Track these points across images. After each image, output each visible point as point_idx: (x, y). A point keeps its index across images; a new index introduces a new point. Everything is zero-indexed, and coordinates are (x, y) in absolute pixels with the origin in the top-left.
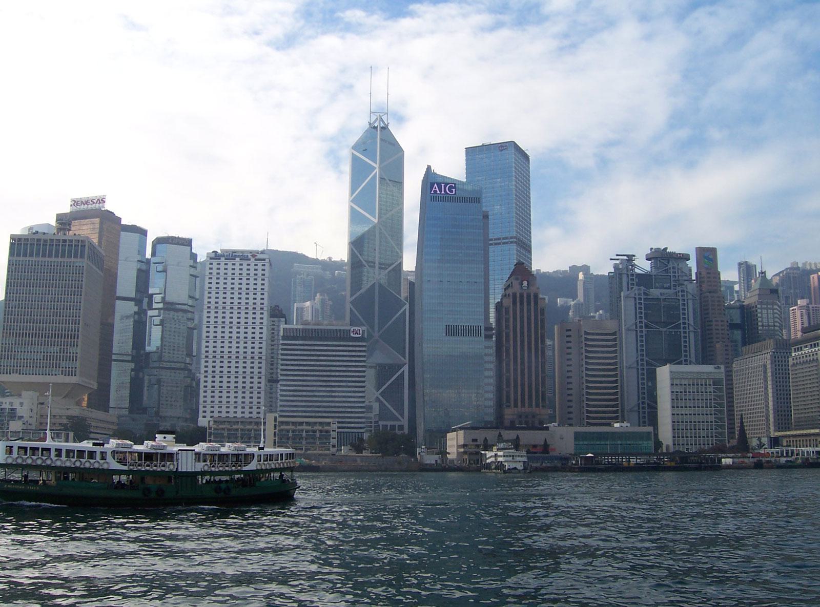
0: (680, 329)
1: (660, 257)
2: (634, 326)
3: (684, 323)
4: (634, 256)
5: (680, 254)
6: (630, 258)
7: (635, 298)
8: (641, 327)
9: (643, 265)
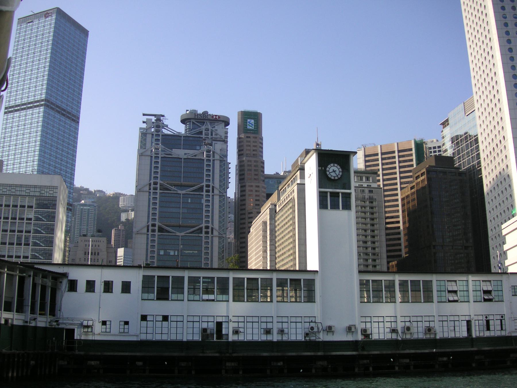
0: (203, 191)
1: (195, 120)
2: (148, 186)
3: (208, 186)
4: (163, 116)
5: (216, 116)
6: (159, 118)
7: (152, 157)
8: (155, 189)
9: (176, 126)
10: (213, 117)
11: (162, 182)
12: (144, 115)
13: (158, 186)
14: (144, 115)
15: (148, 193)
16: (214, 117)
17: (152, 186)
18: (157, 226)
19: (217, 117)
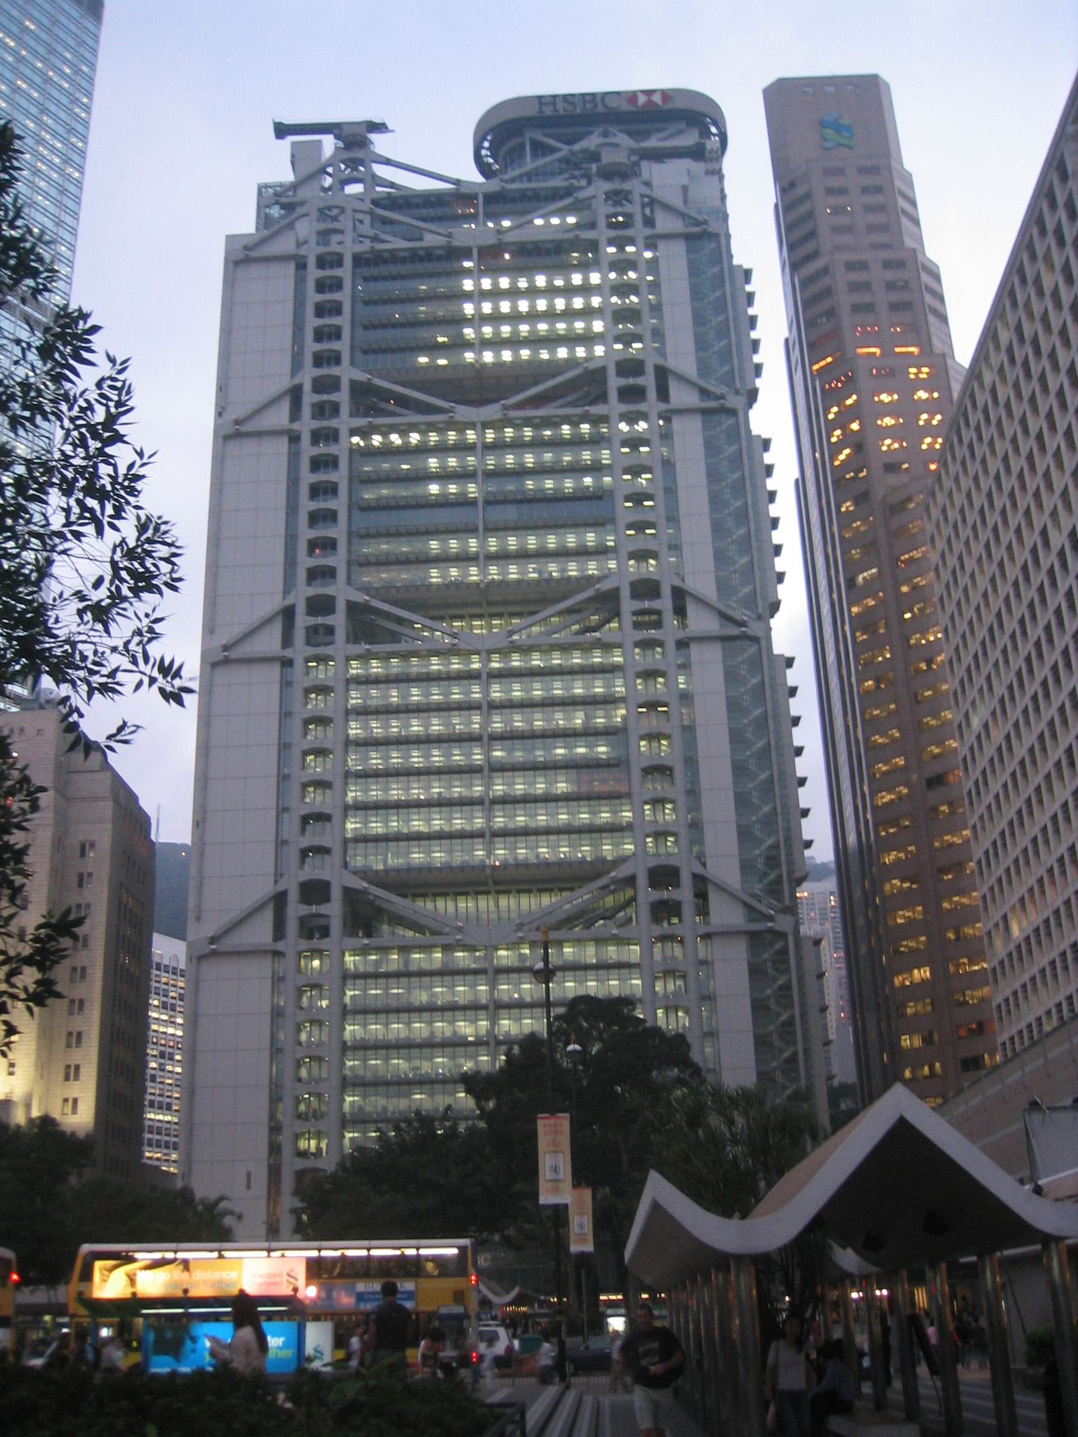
2: (285, 406)
5: (649, 93)
6: (356, 139)
8: (325, 410)
10: (632, 96)
11: (362, 377)
12: (282, 131)
13: (343, 397)
14: (282, 131)
16: (642, 99)
17: (309, 398)
18: (341, 606)
19: (657, 99)
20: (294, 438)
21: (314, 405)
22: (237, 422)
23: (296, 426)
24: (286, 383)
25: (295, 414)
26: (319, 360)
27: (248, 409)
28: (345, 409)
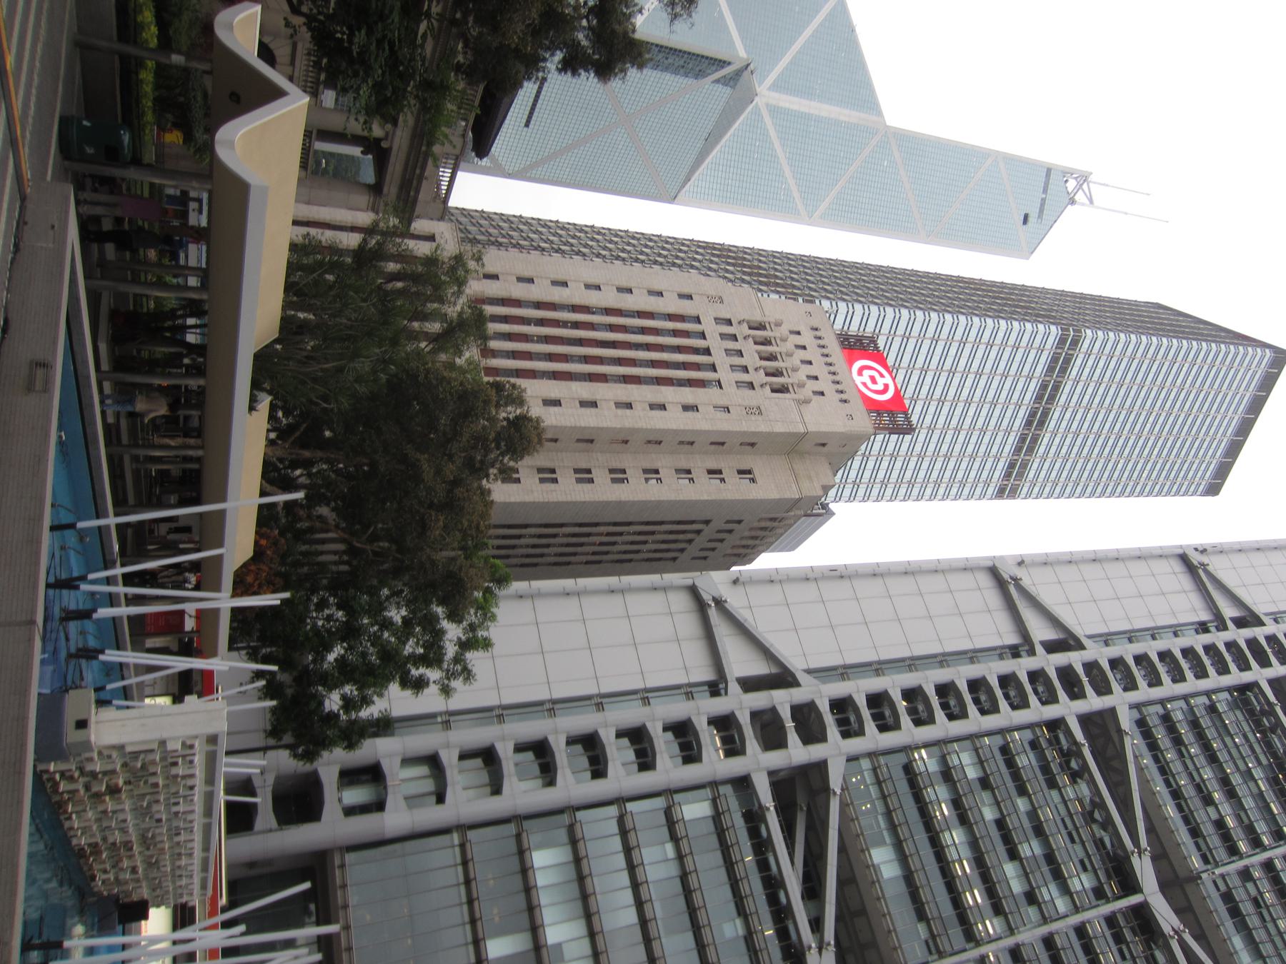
2: (759, 668)
13: (797, 753)
15: (707, 675)
17: (782, 700)
20: (715, 688)
21: (773, 710)
22: (719, 603)
23: (734, 688)
24: (796, 664)
25: (750, 685)
26: (841, 706)
27: (743, 614)
28: (776, 759)
